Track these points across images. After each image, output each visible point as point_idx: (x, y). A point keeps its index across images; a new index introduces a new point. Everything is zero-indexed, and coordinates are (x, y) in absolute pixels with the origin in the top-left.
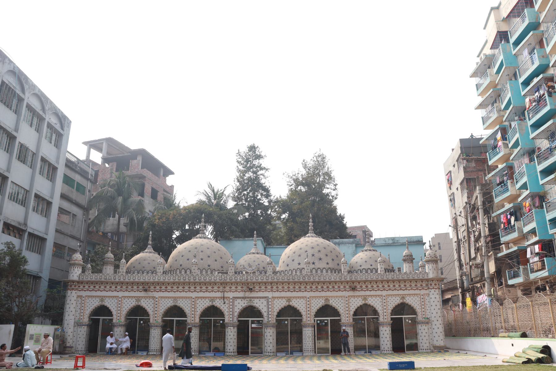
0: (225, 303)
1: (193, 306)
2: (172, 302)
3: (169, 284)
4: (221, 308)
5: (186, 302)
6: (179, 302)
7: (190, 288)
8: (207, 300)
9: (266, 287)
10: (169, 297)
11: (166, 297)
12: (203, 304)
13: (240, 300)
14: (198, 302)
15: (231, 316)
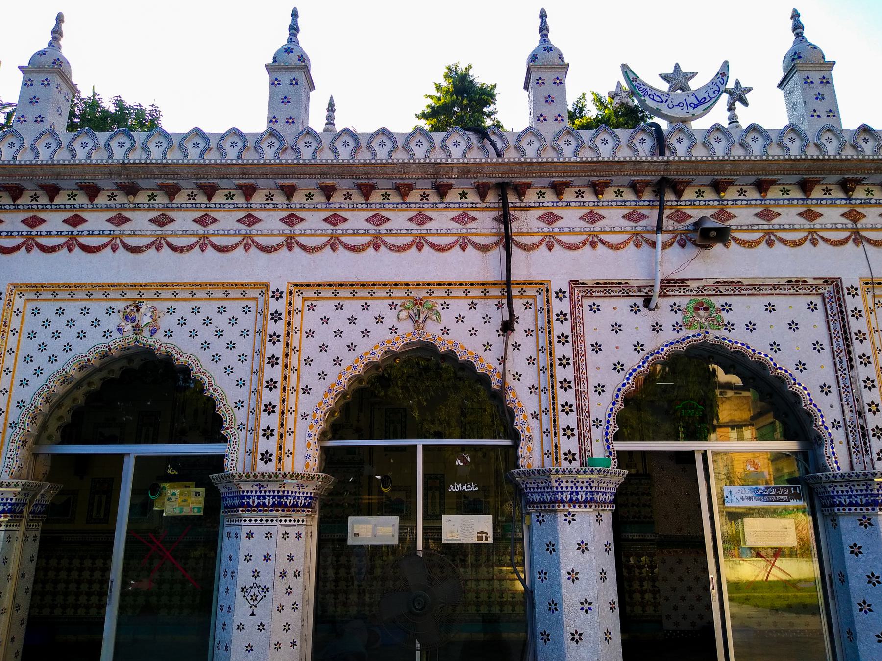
0: (507, 327)
1: (278, 350)
2: (112, 322)
3: (92, 192)
4: (487, 363)
5: (221, 321)
6: (167, 322)
7: (251, 220)
8: (379, 306)
9: (810, 215)
10: (90, 289)
11: (72, 288)
12: (352, 334)
13: (624, 304)
14: (311, 320)
15: (568, 420)
